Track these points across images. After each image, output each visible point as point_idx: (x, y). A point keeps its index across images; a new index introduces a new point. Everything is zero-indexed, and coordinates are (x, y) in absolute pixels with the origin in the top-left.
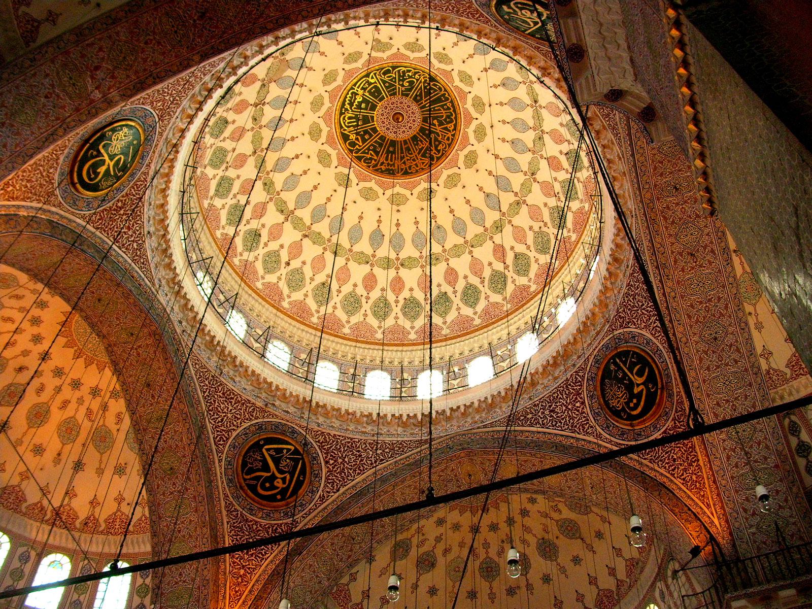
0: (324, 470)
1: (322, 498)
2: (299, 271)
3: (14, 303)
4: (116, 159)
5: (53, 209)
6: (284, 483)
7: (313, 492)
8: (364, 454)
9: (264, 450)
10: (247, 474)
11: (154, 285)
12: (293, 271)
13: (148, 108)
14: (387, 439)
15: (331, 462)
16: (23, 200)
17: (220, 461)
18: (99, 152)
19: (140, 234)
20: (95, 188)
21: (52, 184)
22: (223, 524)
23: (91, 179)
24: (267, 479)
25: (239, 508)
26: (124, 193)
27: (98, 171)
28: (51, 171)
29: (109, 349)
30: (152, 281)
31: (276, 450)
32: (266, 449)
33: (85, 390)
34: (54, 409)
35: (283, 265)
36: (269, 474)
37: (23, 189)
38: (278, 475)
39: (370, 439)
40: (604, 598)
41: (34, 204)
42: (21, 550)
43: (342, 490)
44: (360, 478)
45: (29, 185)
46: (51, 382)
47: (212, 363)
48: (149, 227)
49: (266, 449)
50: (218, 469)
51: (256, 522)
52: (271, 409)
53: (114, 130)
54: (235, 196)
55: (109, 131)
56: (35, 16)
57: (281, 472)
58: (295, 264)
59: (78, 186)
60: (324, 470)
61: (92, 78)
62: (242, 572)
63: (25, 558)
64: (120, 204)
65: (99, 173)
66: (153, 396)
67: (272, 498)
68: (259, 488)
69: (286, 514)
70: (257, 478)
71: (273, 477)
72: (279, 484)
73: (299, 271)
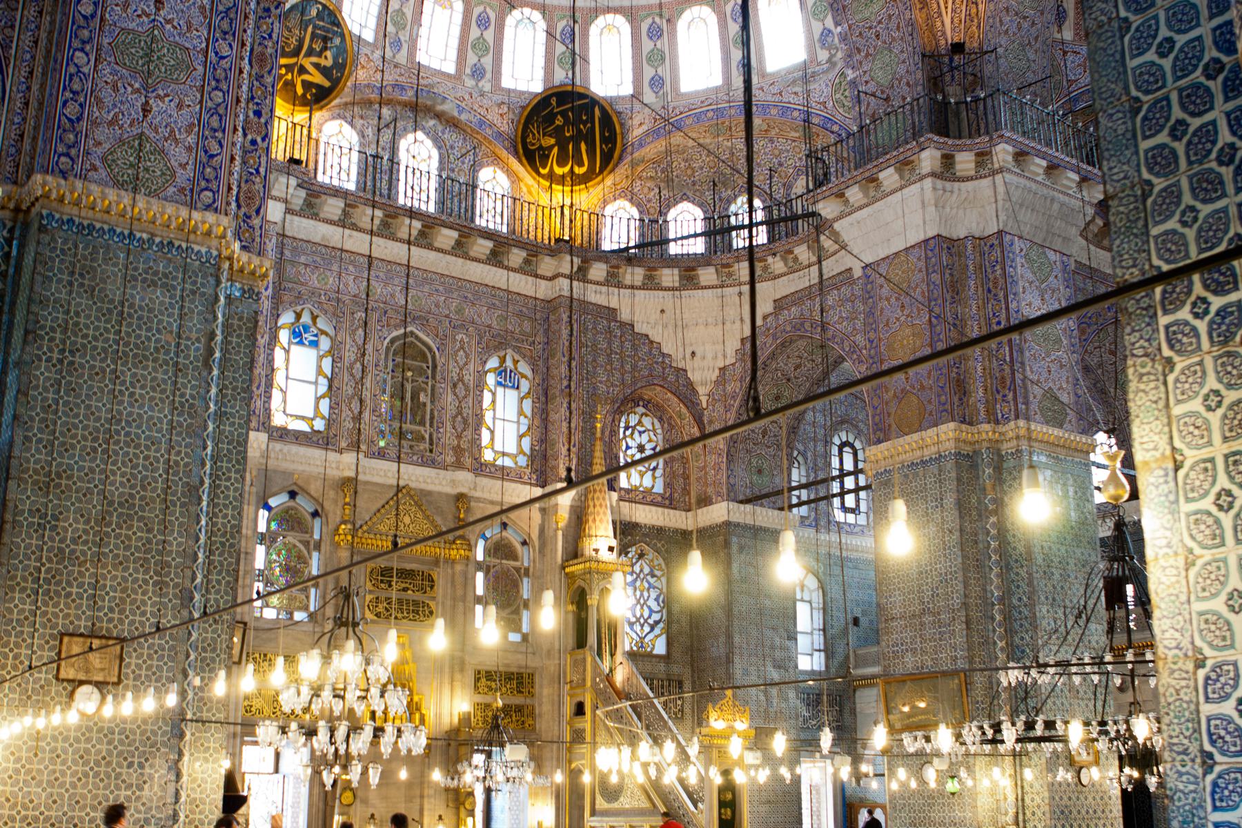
42: (645, 27)
63: (655, 33)
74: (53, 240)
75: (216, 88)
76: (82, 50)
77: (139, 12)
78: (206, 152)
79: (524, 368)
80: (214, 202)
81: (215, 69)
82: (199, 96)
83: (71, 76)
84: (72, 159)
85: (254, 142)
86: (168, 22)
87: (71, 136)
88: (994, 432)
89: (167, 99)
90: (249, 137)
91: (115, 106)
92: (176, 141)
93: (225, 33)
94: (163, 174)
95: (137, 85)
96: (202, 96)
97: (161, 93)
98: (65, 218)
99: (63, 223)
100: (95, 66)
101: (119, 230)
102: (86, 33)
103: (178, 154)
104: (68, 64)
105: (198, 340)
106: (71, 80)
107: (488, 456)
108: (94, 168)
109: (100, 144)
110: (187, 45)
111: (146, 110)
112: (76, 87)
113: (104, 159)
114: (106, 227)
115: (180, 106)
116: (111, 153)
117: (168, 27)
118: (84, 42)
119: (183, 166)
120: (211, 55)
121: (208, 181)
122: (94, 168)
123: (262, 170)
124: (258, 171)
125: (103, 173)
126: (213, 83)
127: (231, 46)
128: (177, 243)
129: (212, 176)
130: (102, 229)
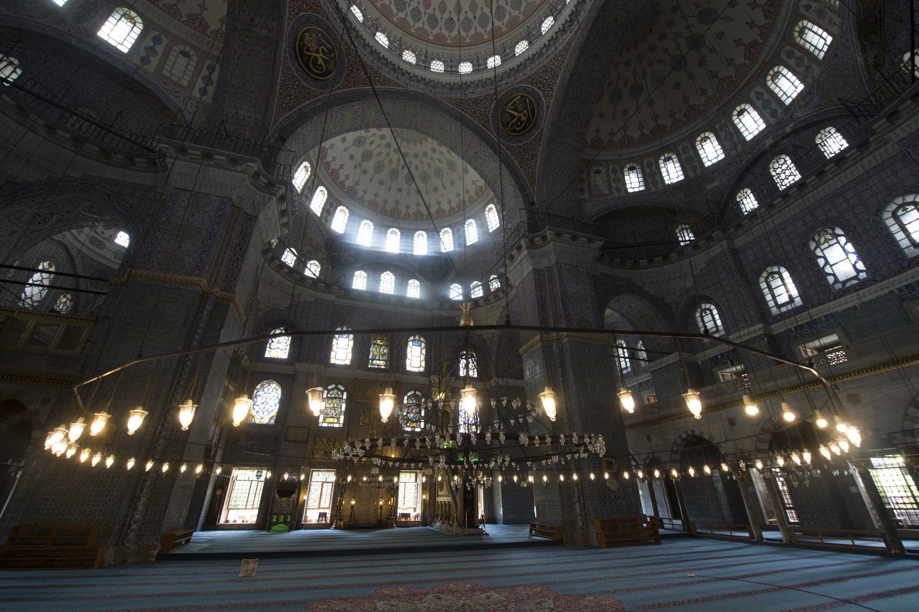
0: (540, 93)
1: (548, 107)
2: (484, 15)
3: (373, 146)
4: (320, 50)
5: (320, 97)
6: (526, 116)
7: (542, 108)
8: (553, 67)
9: (507, 110)
10: (507, 127)
11: (403, 87)
12: (480, 19)
13: (302, 13)
14: (560, 48)
15: (541, 86)
16: (298, 105)
17: (491, 132)
18: (307, 55)
19: (374, 72)
20: (329, 72)
21: (306, 88)
22: (510, 157)
23: (321, 70)
24: (517, 121)
25: (513, 145)
26: (346, 62)
27: (319, 63)
28: (297, 83)
29: (417, 129)
30: (400, 86)
31: (513, 105)
32: (509, 109)
33: (430, 153)
34: (400, 171)
35: (473, 20)
36: (516, 119)
37: (292, 101)
38: (520, 115)
39: (552, 57)
40: (770, 8)
41: (307, 102)
43: (554, 94)
44: (558, 81)
45: (292, 97)
46: (416, 162)
47: (458, 95)
48: (376, 65)
49: (509, 109)
50: (492, 136)
51: (525, 144)
52: (499, 89)
53: (302, 39)
54: (425, 13)
55: (299, 42)
56: (217, 28)
57: (521, 112)
58: (478, 14)
59: (319, 78)
60: (540, 93)
61: (255, 27)
62: (530, 170)
64: (350, 68)
65: (321, 64)
66: (446, 131)
67: (526, 127)
68: (516, 128)
69: (537, 129)
70: (513, 125)
71: (520, 117)
72: (524, 118)
73: (484, 15)
76: (159, 231)
79: (422, 339)
85: (237, 258)
88: (558, 336)
90: (236, 257)
93: (217, 222)
102: (162, 226)
105: (182, 319)
107: (409, 368)
108: (154, 266)
111: (179, 248)
112: (153, 242)
119: (189, 263)
120: (210, 229)
122: (154, 266)
123: (239, 267)
124: (237, 267)
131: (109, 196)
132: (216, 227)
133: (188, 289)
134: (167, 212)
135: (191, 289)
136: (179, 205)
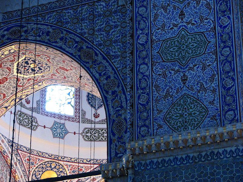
74: (144, 177)
75: (225, 47)
76: (144, 63)
77: (172, 26)
78: (224, 88)
80: (235, 117)
81: (222, 36)
82: (214, 57)
83: (140, 80)
84: (147, 127)
86: (188, 23)
87: (145, 114)
89: (195, 68)
91: (166, 86)
92: (205, 89)
93: (224, 12)
94: (201, 112)
95: (177, 68)
96: (216, 56)
97: (191, 66)
98: (148, 162)
99: (147, 165)
100: (152, 68)
101: (179, 157)
103: (207, 97)
104: (137, 75)
106: (140, 82)
109: (161, 111)
110: (202, 31)
111: (184, 80)
112: (143, 85)
113: (165, 119)
114: (172, 158)
115: (204, 69)
116: (168, 114)
117: (189, 26)
118: (144, 59)
119: (212, 103)
121: (229, 105)
122: (160, 126)
125: (165, 127)
126: (222, 45)
127: (229, 17)
128: (216, 151)
129: (231, 101)
130: (170, 160)
131: (48, 33)
132: (225, 21)
133: (228, 149)
134: (142, 26)
135: (233, 149)
136: (155, 6)
